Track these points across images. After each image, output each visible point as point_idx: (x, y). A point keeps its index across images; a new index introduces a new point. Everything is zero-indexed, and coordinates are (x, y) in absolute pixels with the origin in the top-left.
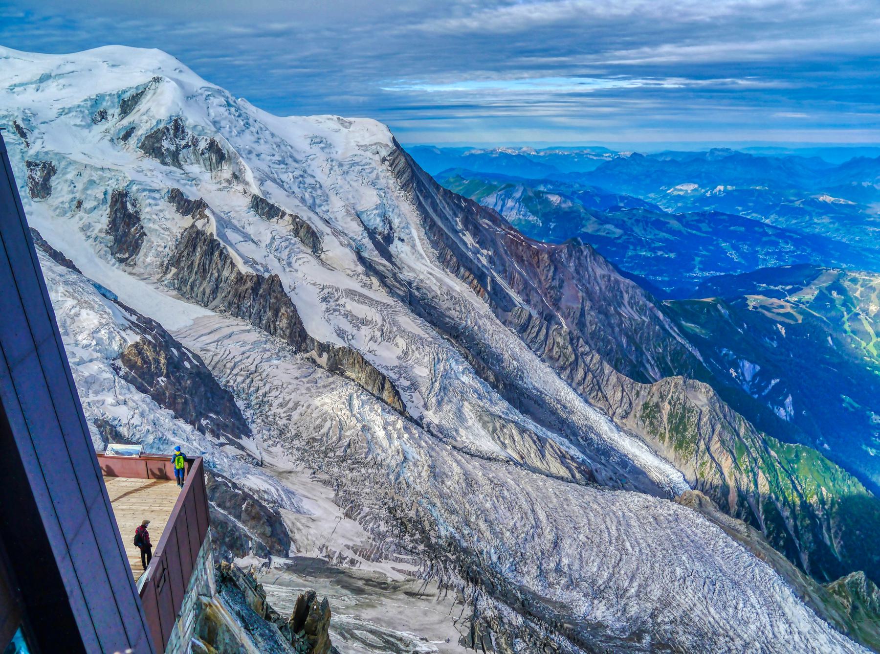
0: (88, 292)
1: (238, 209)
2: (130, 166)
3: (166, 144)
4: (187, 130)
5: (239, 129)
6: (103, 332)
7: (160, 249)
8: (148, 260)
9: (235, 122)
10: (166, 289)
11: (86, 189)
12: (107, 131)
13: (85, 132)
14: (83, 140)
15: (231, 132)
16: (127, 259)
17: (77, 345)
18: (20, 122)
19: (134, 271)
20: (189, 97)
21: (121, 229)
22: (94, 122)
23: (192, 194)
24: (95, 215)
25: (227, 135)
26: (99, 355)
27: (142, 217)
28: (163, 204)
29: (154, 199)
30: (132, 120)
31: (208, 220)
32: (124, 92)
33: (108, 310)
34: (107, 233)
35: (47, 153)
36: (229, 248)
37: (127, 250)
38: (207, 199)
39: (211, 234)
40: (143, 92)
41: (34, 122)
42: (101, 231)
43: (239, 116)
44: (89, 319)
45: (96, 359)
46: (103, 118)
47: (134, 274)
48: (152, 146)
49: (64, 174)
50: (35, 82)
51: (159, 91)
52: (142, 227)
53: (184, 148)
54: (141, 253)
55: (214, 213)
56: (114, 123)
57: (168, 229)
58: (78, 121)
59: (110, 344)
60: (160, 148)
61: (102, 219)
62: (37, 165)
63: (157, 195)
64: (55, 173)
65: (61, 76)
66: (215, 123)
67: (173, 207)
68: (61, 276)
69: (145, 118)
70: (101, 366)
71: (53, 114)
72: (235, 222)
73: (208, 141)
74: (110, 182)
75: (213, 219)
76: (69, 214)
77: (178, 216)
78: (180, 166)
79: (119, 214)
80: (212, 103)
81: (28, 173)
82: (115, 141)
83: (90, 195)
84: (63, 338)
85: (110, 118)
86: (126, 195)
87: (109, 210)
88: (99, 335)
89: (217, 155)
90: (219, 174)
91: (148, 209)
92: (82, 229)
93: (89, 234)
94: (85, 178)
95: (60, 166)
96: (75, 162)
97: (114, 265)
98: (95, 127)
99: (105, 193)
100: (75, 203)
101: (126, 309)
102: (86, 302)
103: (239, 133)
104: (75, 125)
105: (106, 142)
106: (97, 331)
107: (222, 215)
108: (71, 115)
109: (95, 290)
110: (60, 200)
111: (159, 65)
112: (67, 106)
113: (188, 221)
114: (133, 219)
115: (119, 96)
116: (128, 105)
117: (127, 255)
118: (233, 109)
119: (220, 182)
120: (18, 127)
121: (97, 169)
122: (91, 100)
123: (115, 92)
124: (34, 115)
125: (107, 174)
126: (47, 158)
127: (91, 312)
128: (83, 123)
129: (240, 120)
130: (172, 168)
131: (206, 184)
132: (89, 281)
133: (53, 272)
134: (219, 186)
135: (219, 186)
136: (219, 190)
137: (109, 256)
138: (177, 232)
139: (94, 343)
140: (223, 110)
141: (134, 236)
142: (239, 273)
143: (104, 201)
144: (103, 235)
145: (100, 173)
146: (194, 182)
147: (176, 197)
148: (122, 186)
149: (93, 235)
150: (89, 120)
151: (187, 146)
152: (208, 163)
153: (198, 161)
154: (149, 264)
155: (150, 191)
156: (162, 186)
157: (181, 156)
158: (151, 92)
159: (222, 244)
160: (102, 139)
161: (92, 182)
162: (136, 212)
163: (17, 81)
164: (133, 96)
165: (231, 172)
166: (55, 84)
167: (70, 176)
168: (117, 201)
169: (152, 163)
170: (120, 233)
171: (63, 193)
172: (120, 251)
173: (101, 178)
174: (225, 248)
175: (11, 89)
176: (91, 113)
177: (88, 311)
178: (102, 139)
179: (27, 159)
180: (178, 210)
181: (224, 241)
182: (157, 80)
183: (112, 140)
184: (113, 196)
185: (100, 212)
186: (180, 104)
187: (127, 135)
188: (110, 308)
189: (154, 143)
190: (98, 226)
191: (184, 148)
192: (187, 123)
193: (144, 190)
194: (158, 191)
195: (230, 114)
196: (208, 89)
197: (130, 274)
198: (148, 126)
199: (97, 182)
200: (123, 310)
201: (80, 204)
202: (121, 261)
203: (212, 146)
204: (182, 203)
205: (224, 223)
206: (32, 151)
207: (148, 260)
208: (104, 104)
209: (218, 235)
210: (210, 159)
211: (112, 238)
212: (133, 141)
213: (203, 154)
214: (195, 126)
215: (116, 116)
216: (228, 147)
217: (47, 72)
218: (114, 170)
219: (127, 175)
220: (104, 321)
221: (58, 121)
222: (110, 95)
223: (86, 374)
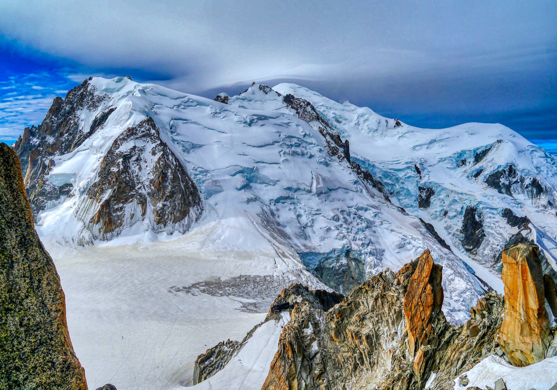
0: (460, 267)
1: (551, 226)
2: (479, 193)
3: (502, 180)
4: (517, 172)
5: (553, 173)
6: (468, 293)
7: (494, 246)
8: (486, 252)
9: (550, 168)
10: (497, 273)
11: (450, 204)
12: (465, 171)
13: (452, 172)
14: (451, 177)
15: (548, 174)
16: (471, 250)
17: (451, 298)
18: (418, 166)
19: (475, 258)
20: (520, 151)
21: (470, 230)
22: (458, 166)
23: (519, 213)
24: (455, 220)
25: (545, 176)
26: (464, 308)
27: (484, 225)
28: (499, 218)
29: (493, 214)
30: (481, 165)
31: (531, 231)
32: (478, 149)
33: (472, 281)
34: (461, 232)
35: (430, 183)
36: (545, 252)
37: (472, 244)
38: (529, 217)
39: (533, 241)
40: (490, 149)
41: (425, 166)
42: (457, 230)
43: (554, 164)
44: (460, 284)
45: (462, 310)
46: (463, 164)
47: (476, 260)
48: (493, 181)
49: (439, 195)
50: (427, 144)
51: (500, 148)
52: (483, 231)
53: (514, 183)
54: (481, 247)
55: (535, 227)
56: (470, 167)
57: (501, 234)
58: (449, 166)
59: (471, 302)
60: (499, 183)
61: (458, 224)
62: (424, 189)
63: (495, 212)
64: (433, 194)
65: (441, 140)
66: (537, 168)
67: (505, 220)
68: (446, 254)
69: (490, 164)
70: (466, 316)
71: (435, 161)
72: (549, 234)
73: (532, 180)
74: (466, 201)
75: (534, 231)
76: (438, 219)
77: (508, 226)
78: (511, 195)
79: (469, 221)
80: (535, 155)
81: (419, 193)
82: (470, 177)
83: (453, 208)
84: (444, 292)
85: (467, 164)
86: (475, 210)
87: (463, 218)
88: (464, 295)
89: (537, 188)
90: (538, 201)
91: (488, 220)
92: (447, 228)
93: (450, 231)
94: (451, 199)
95: (437, 190)
96: (446, 189)
97: (463, 252)
98: (458, 169)
99: (462, 208)
100: (443, 212)
101: (482, 281)
102: (459, 273)
103: (553, 175)
104: (447, 168)
105: (464, 177)
106: (464, 292)
107: (540, 228)
108: (445, 162)
109: (465, 267)
110: (435, 210)
111: (500, 133)
112: (444, 157)
113: (515, 230)
114: (478, 225)
115: (475, 151)
116: (479, 156)
117: (471, 247)
118: (549, 160)
119: (538, 207)
120: (417, 168)
121: (458, 193)
122: (458, 153)
123: (472, 149)
124: (426, 162)
125: (464, 197)
126: (430, 186)
127: (461, 280)
128: (452, 167)
129: (554, 166)
130: (505, 195)
131: (526, 206)
132: (460, 260)
133: (442, 251)
134: (537, 209)
135: (537, 209)
136: (538, 212)
137: (461, 247)
138: (507, 237)
139: (462, 299)
140: (542, 160)
141: (477, 236)
142: (552, 270)
143: (461, 213)
144: (458, 233)
145: (460, 196)
146: (520, 205)
147: (508, 214)
148: (473, 204)
149: (452, 232)
150: (455, 165)
151: (516, 182)
152: (530, 194)
153: (523, 192)
154: (486, 255)
155: (491, 209)
156: (499, 206)
157: (512, 188)
158: (495, 149)
159: (540, 248)
160: (462, 176)
161: (455, 201)
162: (481, 221)
163: (418, 143)
164: (483, 151)
165: (547, 201)
166: (438, 145)
167: (442, 197)
168: (469, 213)
169: (493, 192)
170: (469, 233)
171: (437, 206)
172: (468, 244)
173: (460, 199)
174: (542, 251)
175: (414, 148)
176: (457, 161)
177: (459, 278)
178: (462, 176)
179: (419, 185)
180: (508, 223)
181: (541, 246)
182: (499, 141)
183: (468, 177)
184: (467, 210)
185: (458, 219)
186: (514, 156)
187: (478, 174)
188: (473, 279)
189: (494, 180)
190: (456, 228)
191: (514, 183)
192: (518, 167)
193: (487, 208)
194: (496, 209)
195: (547, 162)
196: (532, 147)
197: (473, 259)
198: (492, 169)
199: (458, 201)
200: (480, 282)
201: (446, 213)
202: (468, 250)
203: (535, 183)
204: (512, 218)
205: (541, 234)
206: (422, 182)
207: (486, 252)
208: (465, 156)
209: (537, 241)
210: (532, 191)
211: (463, 235)
212: (481, 178)
213: (527, 187)
214: (524, 170)
215: (472, 163)
216: (545, 183)
217: (434, 138)
218: (469, 195)
219: (477, 198)
220: (469, 287)
221: (438, 165)
222: (469, 151)
223: (457, 319)
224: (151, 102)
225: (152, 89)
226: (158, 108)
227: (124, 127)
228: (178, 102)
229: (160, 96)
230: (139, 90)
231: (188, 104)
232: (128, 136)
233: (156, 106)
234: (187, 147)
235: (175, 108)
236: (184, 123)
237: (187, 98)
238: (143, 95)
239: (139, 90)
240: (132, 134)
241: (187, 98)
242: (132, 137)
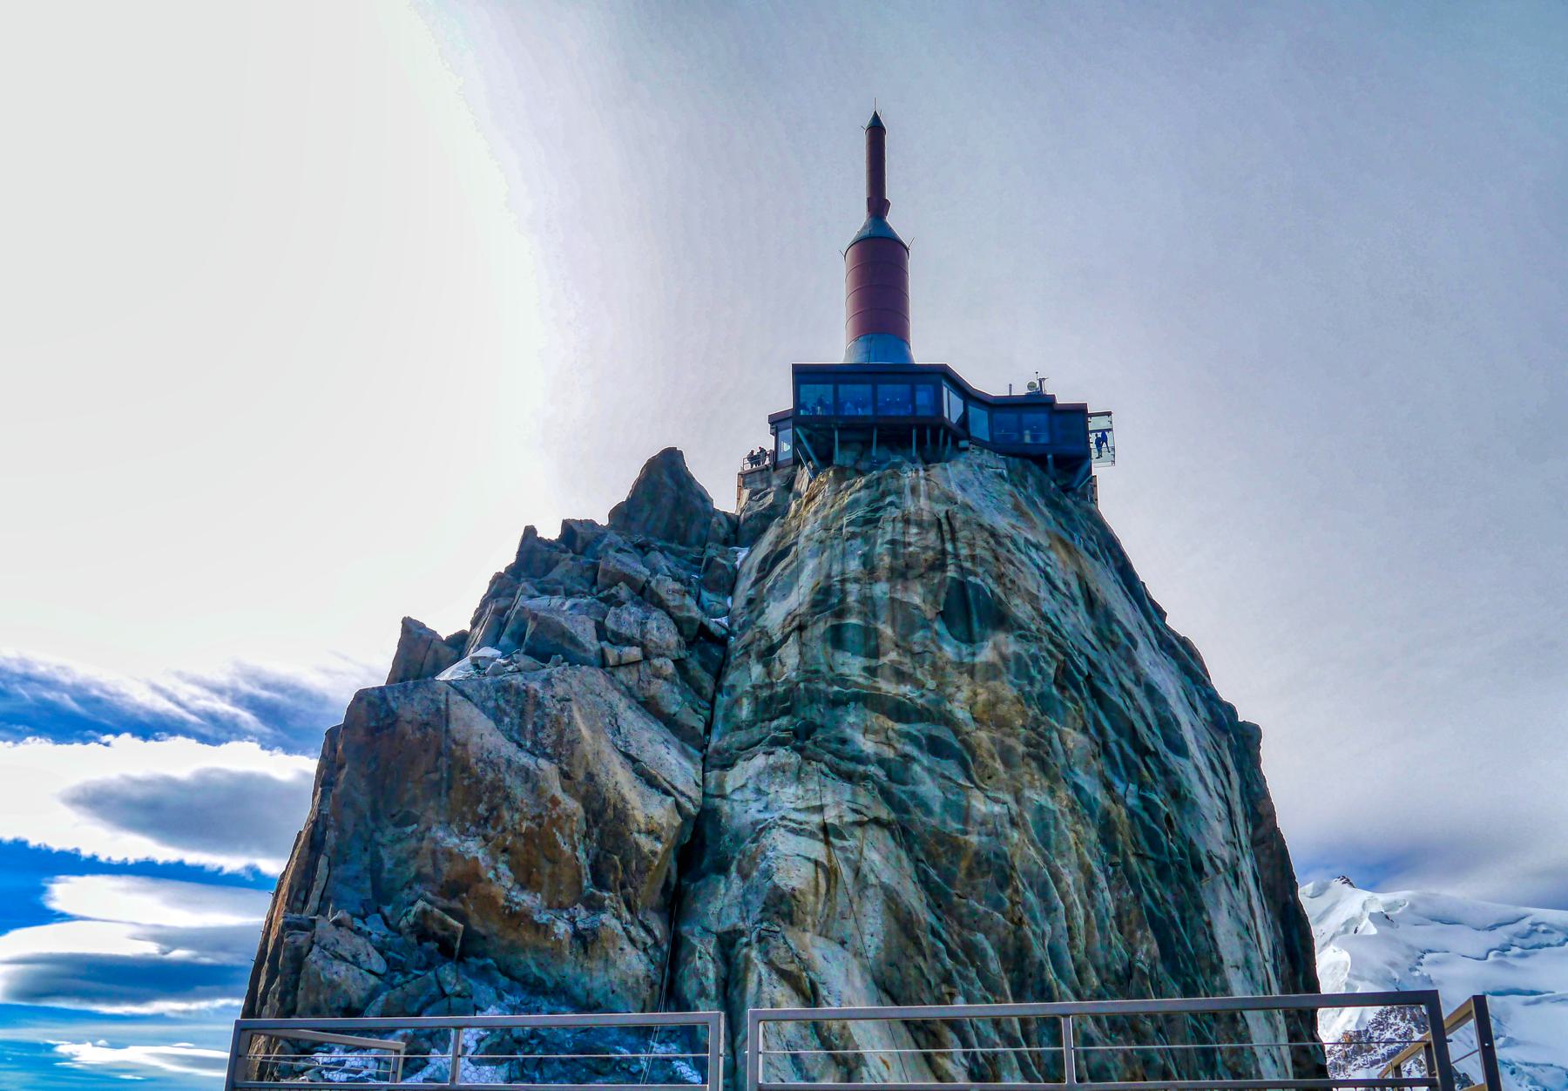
224: (1410, 947)
225: (1412, 907)
226: (1436, 963)
227: (1333, 1030)
228: (1501, 936)
229: (1438, 925)
230: (1372, 917)
231: (1535, 939)
232: (1346, 1057)
233: (1428, 957)
234: (1546, 1082)
235: (1491, 957)
236: (1527, 1004)
237: (1528, 921)
238: (1384, 928)
239: (1372, 917)
240: (1358, 1052)
241: (1528, 921)
242: (1360, 1061)
